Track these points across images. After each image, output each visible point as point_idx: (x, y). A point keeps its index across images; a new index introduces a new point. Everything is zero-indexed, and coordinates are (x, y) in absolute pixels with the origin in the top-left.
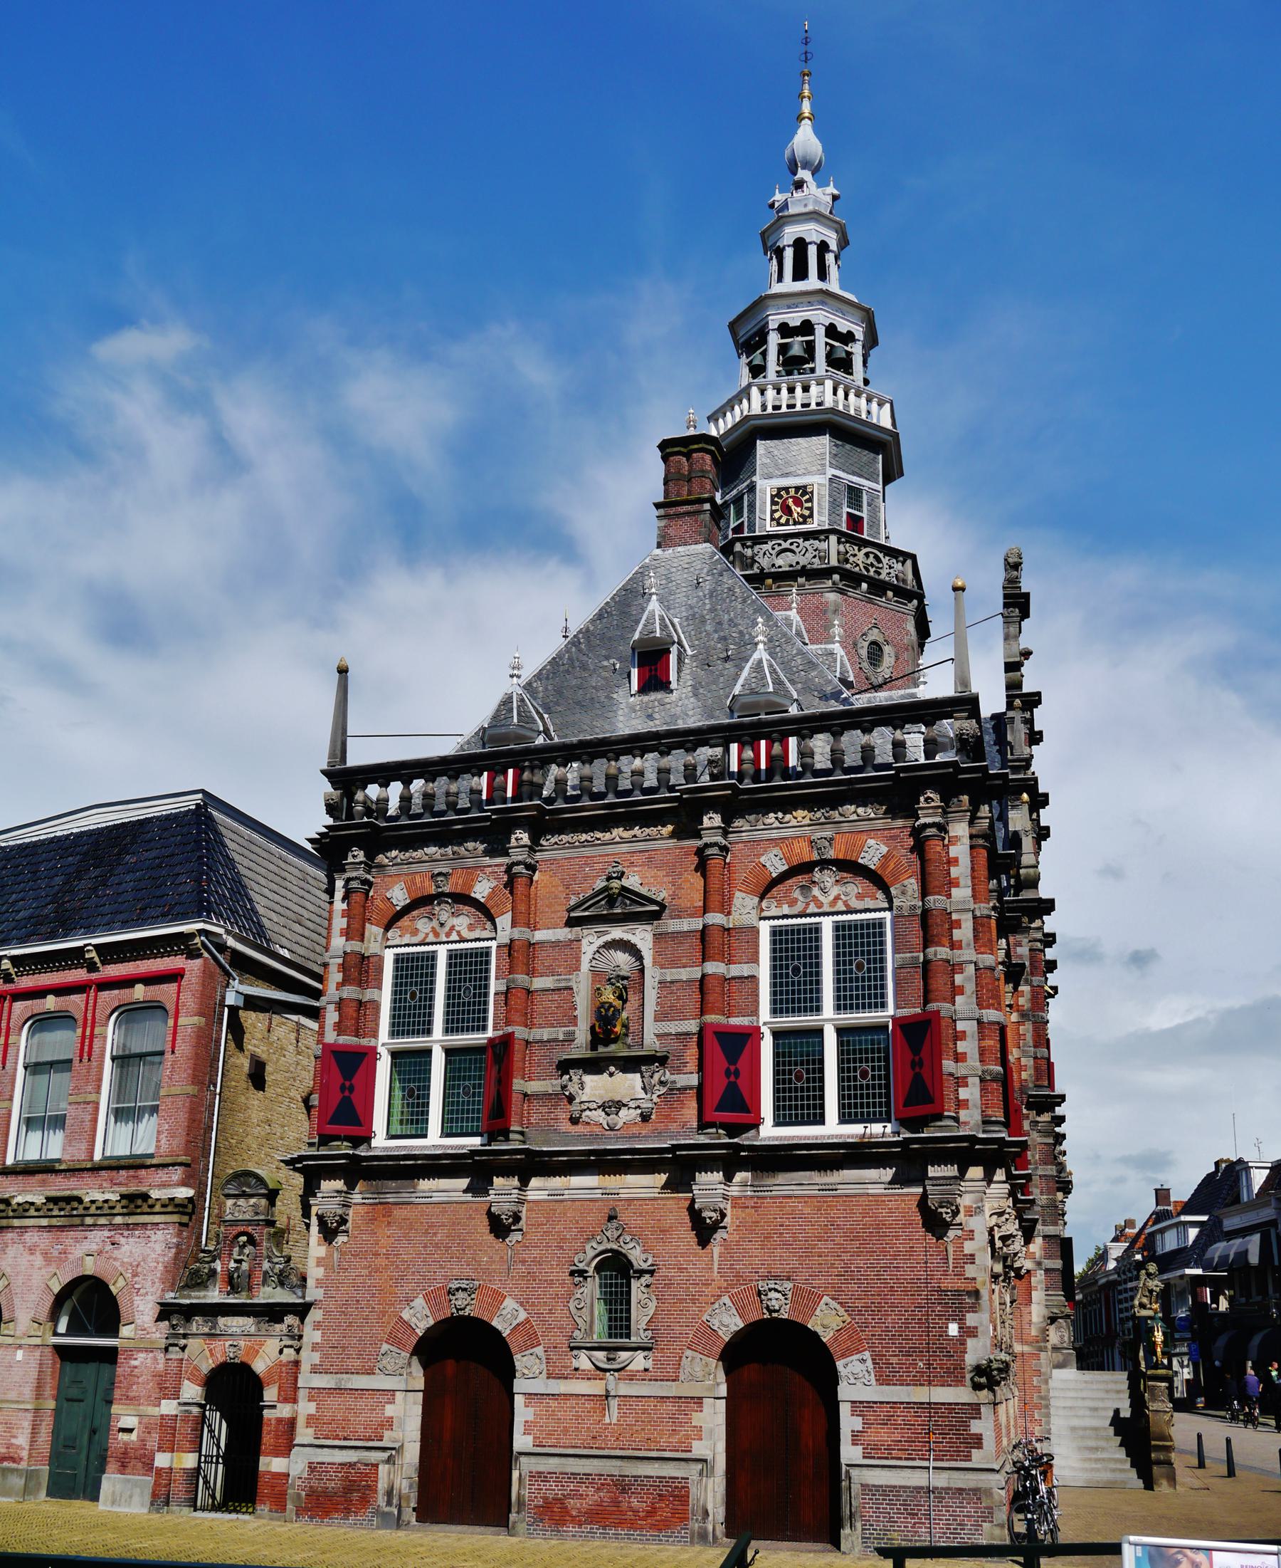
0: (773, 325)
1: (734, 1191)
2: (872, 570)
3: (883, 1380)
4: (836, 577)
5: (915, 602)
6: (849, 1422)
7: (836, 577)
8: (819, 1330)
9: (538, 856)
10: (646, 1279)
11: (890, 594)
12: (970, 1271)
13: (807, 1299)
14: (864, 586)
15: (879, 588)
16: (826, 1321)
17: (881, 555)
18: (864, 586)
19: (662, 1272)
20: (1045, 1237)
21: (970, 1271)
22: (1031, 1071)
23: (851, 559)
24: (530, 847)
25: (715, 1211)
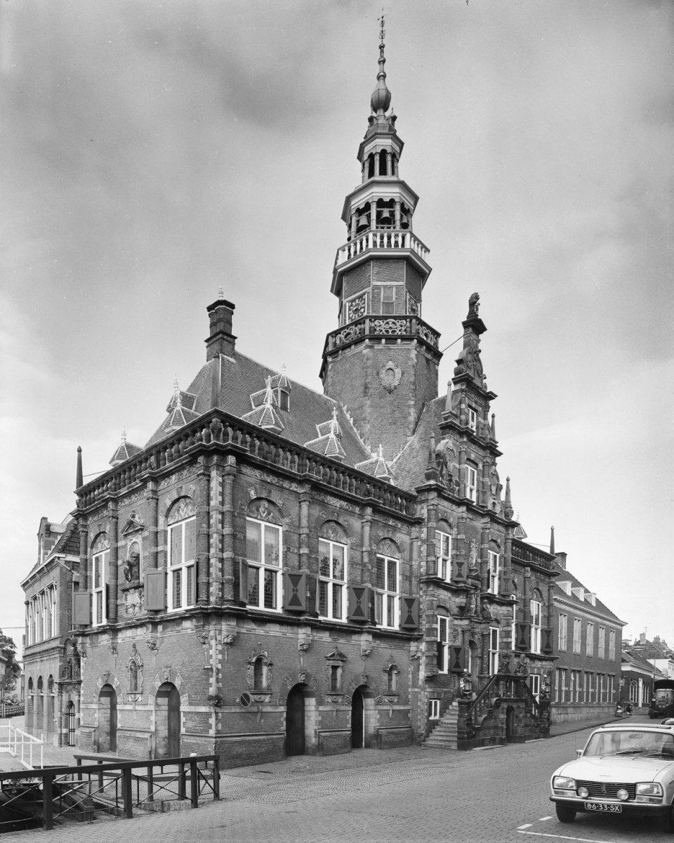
0: (353, 212)
1: (159, 635)
2: (390, 331)
3: (190, 704)
4: (367, 341)
5: (415, 341)
6: (183, 719)
7: (367, 341)
8: (176, 685)
9: (119, 512)
10: (141, 670)
11: (399, 341)
12: (212, 661)
13: (173, 673)
14: (383, 341)
15: (391, 339)
16: (177, 683)
17: (396, 322)
18: (383, 341)
19: (144, 667)
20: (427, 642)
21: (212, 661)
22: (425, 568)
23: (378, 329)
24: (113, 510)
25: (149, 643)
